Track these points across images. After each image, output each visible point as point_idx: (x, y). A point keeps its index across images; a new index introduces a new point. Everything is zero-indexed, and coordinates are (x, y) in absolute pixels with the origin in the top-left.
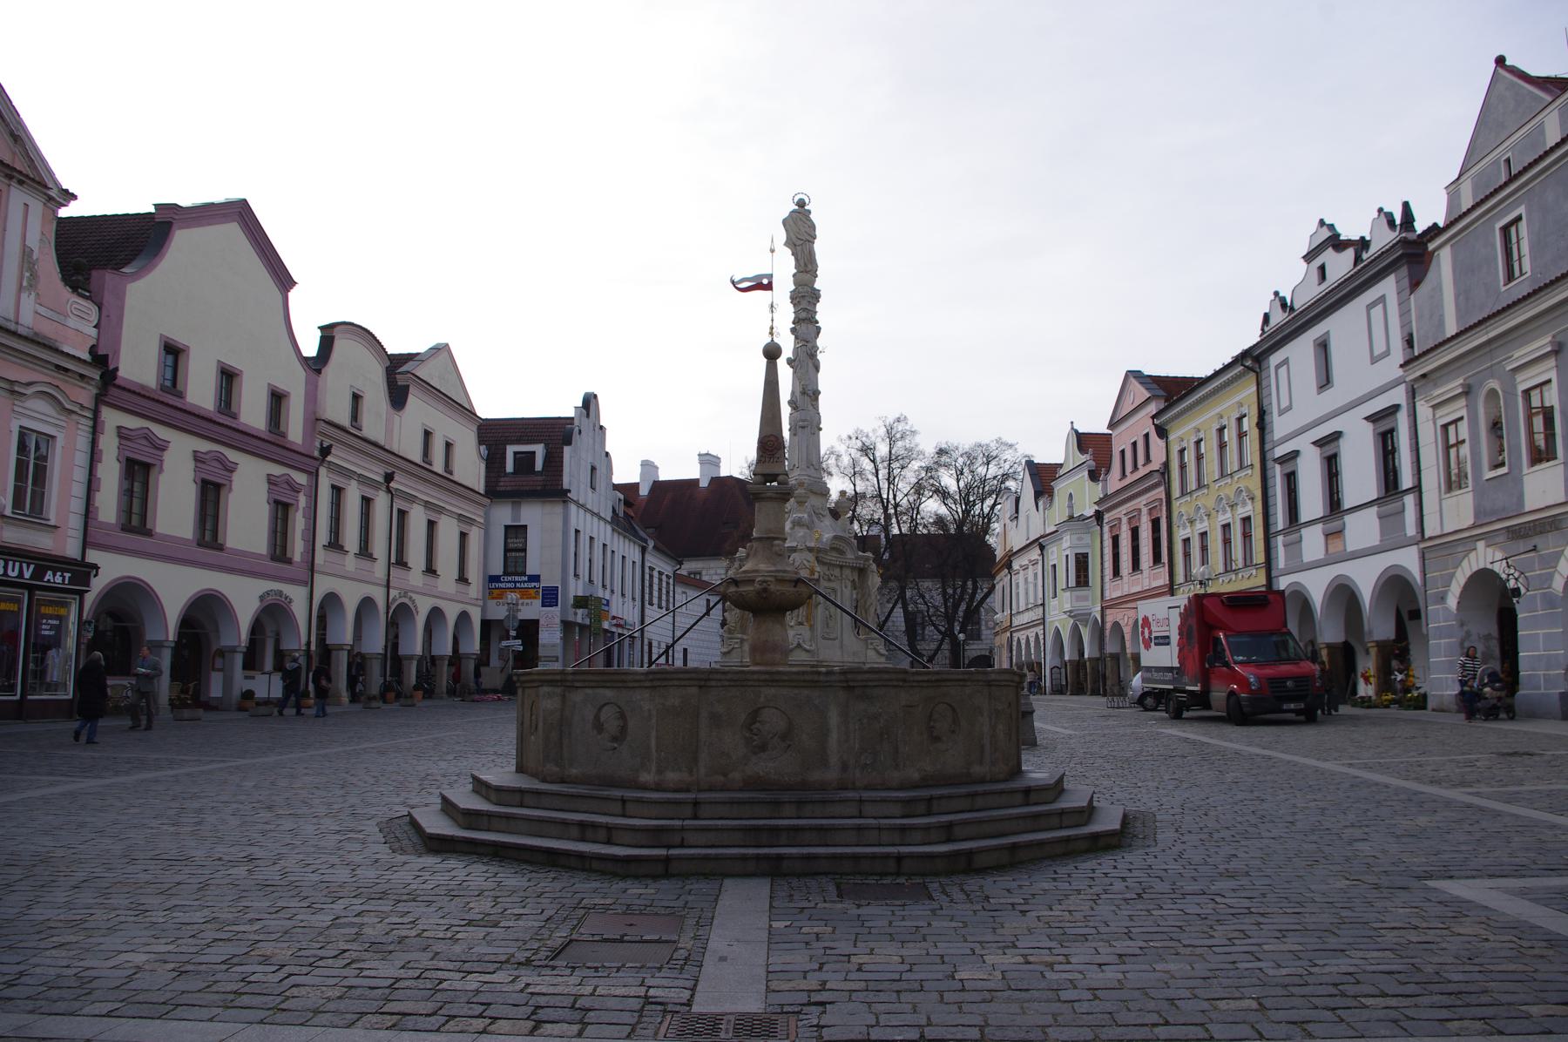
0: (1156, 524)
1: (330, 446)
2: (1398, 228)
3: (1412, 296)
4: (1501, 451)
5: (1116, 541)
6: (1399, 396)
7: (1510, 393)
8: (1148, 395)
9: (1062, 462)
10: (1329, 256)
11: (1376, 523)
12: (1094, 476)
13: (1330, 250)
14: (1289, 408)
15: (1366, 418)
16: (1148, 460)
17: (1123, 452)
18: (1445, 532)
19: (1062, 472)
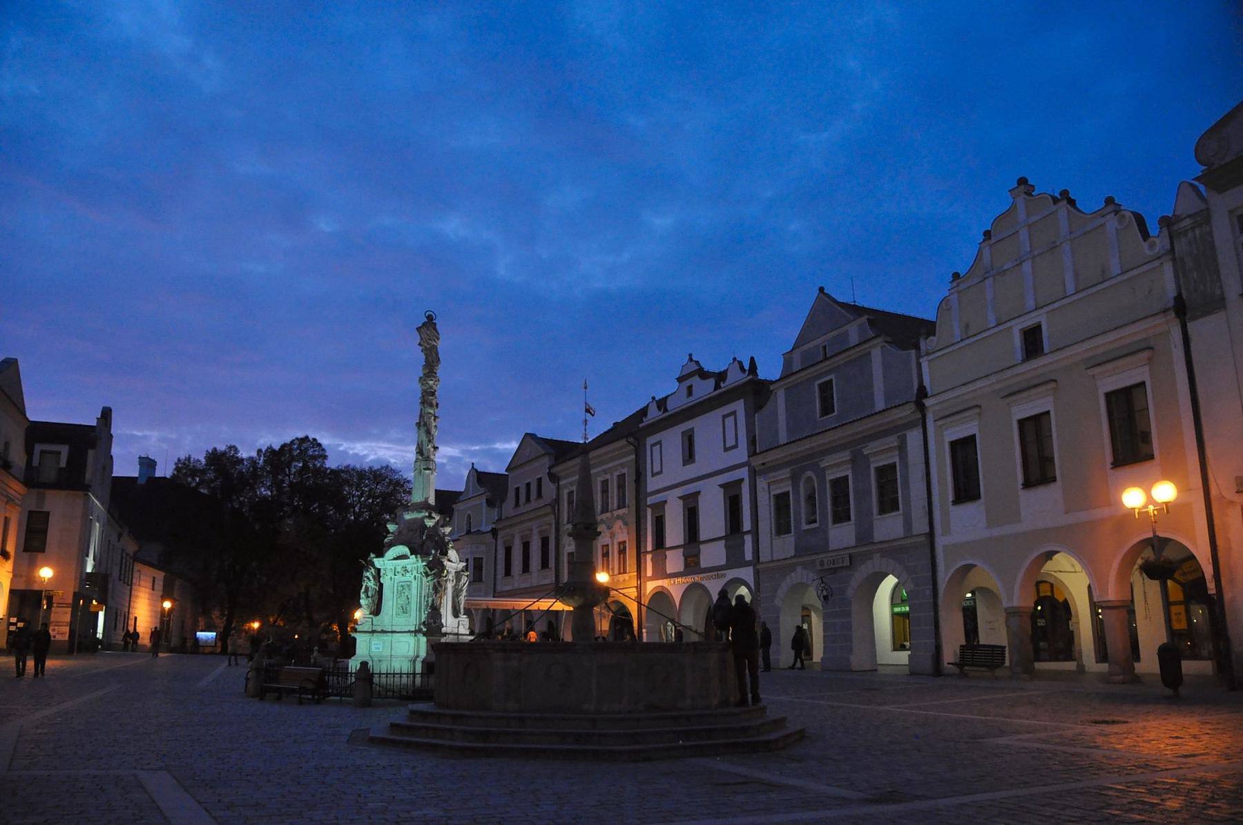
0: (545, 542)
2: (747, 372)
8: (543, 453)
9: (463, 490)
10: (695, 380)
11: (723, 552)
12: (490, 503)
14: (660, 472)
15: (720, 486)
16: (539, 495)
17: (517, 489)
18: (775, 559)
19: (461, 498)
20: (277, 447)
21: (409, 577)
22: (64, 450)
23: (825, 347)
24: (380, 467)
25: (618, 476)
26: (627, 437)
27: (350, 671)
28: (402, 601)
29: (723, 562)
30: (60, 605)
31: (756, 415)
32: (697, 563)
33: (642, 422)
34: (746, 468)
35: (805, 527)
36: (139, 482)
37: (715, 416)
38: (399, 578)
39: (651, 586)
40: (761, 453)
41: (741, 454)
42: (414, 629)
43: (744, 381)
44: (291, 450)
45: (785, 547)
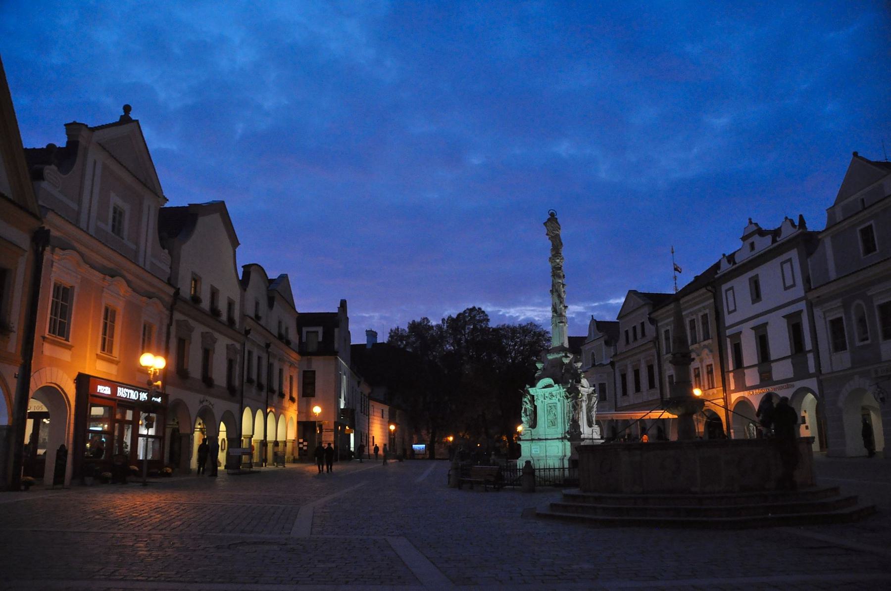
0: (650, 368)
1: (250, 330)
2: (798, 227)
3: (809, 260)
4: (865, 332)
5: (624, 377)
8: (644, 303)
9: (587, 336)
10: (756, 239)
12: (607, 343)
13: (757, 235)
14: (735, 310)
16: (643, 334)
17: (627, 332)
19: (587, 341)
20: (454, 316)
21: (555, 400)
22: (320, 330)
24: (526, 324)
25: (702, 316)
26: (705, 286)
27: (518, 468)
28: (551, 417)
29: (791, 375)
30: (328, 430)
32: (770, 377)
33: (717, 274)
34: (804, 302)
35: (858, 343)
36: (367, 347)
37: (776, 262)
38: (547, 401)
39: (734, 397)
40: (813, 289)
41: (799, 291)
42: (561, 437)
43: (795, 234)
44: (464, 317)
45: (843, 360)
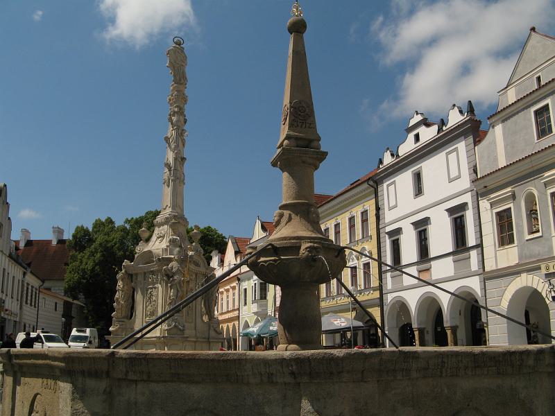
6: (467, 198)
7: (543, 194)
13: (424, 127)
14: (396, 206)
23: (539, 78)
31: (476, 148)
41: (465, 182)
45: (510, 256)
